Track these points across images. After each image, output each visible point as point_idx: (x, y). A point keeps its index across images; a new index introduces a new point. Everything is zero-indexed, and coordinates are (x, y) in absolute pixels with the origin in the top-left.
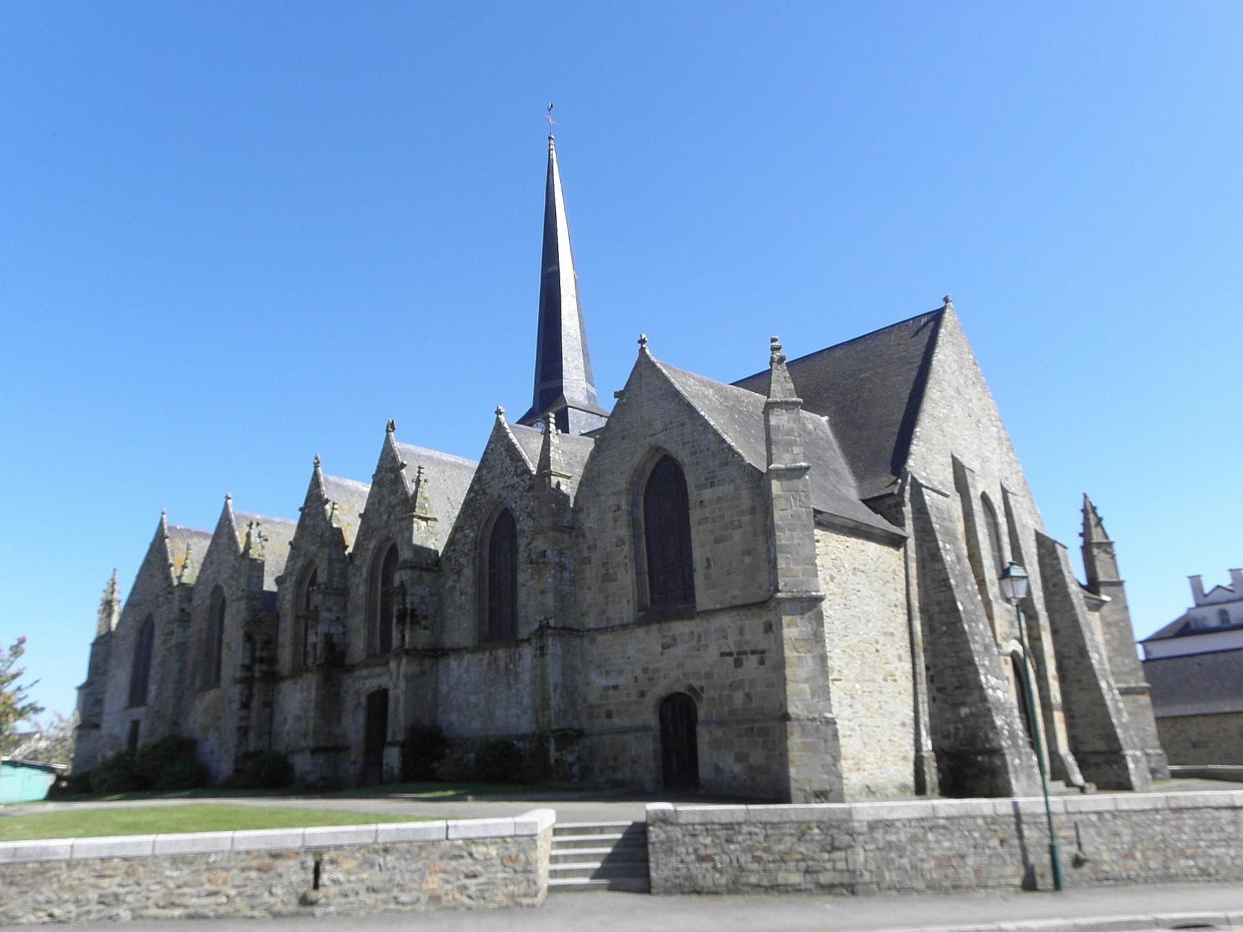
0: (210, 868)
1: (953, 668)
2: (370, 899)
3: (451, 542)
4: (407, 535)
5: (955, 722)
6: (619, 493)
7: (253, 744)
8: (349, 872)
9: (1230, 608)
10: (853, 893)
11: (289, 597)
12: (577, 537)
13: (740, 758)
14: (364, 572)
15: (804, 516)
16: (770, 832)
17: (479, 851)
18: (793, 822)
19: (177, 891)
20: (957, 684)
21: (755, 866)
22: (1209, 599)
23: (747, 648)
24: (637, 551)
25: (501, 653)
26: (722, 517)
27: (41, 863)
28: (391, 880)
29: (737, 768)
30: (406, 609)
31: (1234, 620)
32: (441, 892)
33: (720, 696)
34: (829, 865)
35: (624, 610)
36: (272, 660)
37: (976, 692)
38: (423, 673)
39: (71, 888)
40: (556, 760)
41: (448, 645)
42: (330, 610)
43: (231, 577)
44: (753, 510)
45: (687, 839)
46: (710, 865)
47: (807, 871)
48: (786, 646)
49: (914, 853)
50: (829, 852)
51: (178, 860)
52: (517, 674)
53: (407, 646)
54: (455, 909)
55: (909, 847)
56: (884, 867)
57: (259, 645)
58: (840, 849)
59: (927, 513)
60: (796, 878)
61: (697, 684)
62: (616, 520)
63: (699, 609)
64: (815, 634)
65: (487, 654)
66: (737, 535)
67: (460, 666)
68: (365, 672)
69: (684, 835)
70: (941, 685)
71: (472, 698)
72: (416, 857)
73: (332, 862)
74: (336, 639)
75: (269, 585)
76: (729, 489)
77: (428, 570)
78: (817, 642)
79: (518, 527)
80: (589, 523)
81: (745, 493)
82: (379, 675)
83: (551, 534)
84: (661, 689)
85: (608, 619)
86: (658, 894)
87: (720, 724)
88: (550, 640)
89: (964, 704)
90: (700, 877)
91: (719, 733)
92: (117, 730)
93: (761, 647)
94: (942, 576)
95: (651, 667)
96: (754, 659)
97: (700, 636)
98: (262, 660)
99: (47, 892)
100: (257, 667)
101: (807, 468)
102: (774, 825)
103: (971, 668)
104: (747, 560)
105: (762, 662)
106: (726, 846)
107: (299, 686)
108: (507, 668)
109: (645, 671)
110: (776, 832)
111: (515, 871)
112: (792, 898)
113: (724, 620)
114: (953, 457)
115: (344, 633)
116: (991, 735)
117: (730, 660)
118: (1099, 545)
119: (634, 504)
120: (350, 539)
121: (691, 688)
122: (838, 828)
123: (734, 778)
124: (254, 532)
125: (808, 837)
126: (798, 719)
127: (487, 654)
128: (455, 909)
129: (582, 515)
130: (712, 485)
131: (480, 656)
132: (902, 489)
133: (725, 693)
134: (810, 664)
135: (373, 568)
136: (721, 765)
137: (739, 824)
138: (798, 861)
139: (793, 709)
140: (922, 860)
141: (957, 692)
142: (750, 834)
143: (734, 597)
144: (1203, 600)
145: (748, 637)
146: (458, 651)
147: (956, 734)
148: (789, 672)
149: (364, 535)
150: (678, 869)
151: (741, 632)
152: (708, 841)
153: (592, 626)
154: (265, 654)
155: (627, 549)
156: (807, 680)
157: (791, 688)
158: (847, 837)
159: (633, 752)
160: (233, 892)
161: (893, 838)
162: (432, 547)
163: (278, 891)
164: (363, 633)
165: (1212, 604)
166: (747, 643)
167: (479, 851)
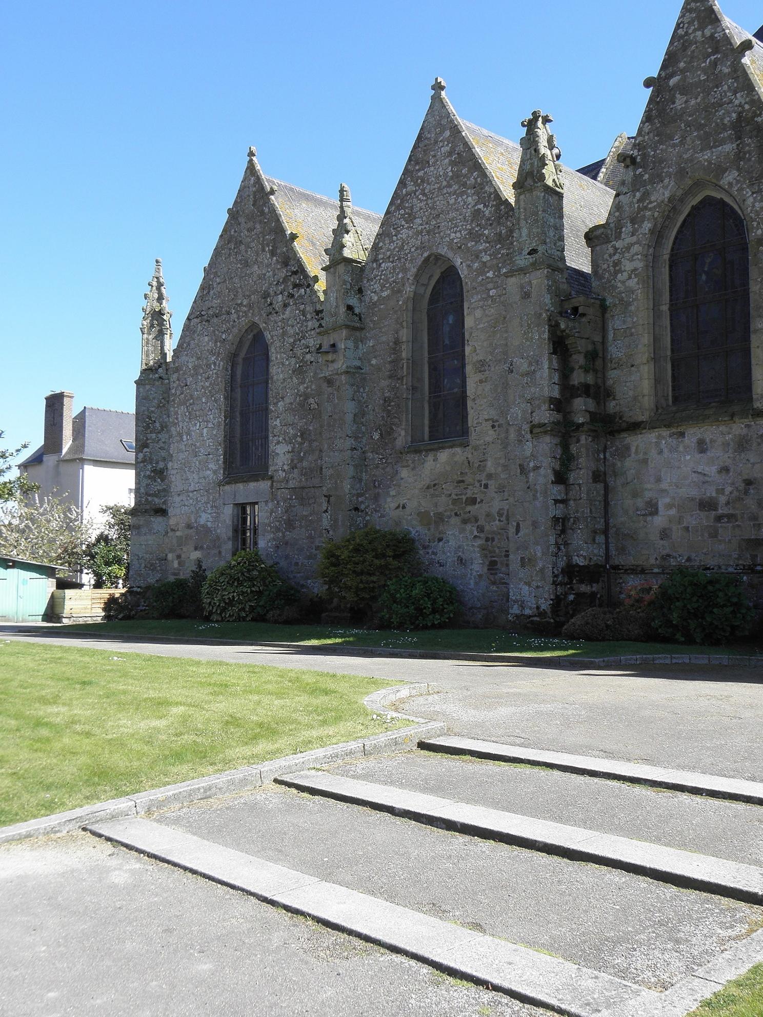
7: (584, 551)
36: (600, 392)
43: (474, 236)
57: (578, 360)
92: (205, 518)
98: (586, 390)
124: (542, 133)
154: (590, 379)
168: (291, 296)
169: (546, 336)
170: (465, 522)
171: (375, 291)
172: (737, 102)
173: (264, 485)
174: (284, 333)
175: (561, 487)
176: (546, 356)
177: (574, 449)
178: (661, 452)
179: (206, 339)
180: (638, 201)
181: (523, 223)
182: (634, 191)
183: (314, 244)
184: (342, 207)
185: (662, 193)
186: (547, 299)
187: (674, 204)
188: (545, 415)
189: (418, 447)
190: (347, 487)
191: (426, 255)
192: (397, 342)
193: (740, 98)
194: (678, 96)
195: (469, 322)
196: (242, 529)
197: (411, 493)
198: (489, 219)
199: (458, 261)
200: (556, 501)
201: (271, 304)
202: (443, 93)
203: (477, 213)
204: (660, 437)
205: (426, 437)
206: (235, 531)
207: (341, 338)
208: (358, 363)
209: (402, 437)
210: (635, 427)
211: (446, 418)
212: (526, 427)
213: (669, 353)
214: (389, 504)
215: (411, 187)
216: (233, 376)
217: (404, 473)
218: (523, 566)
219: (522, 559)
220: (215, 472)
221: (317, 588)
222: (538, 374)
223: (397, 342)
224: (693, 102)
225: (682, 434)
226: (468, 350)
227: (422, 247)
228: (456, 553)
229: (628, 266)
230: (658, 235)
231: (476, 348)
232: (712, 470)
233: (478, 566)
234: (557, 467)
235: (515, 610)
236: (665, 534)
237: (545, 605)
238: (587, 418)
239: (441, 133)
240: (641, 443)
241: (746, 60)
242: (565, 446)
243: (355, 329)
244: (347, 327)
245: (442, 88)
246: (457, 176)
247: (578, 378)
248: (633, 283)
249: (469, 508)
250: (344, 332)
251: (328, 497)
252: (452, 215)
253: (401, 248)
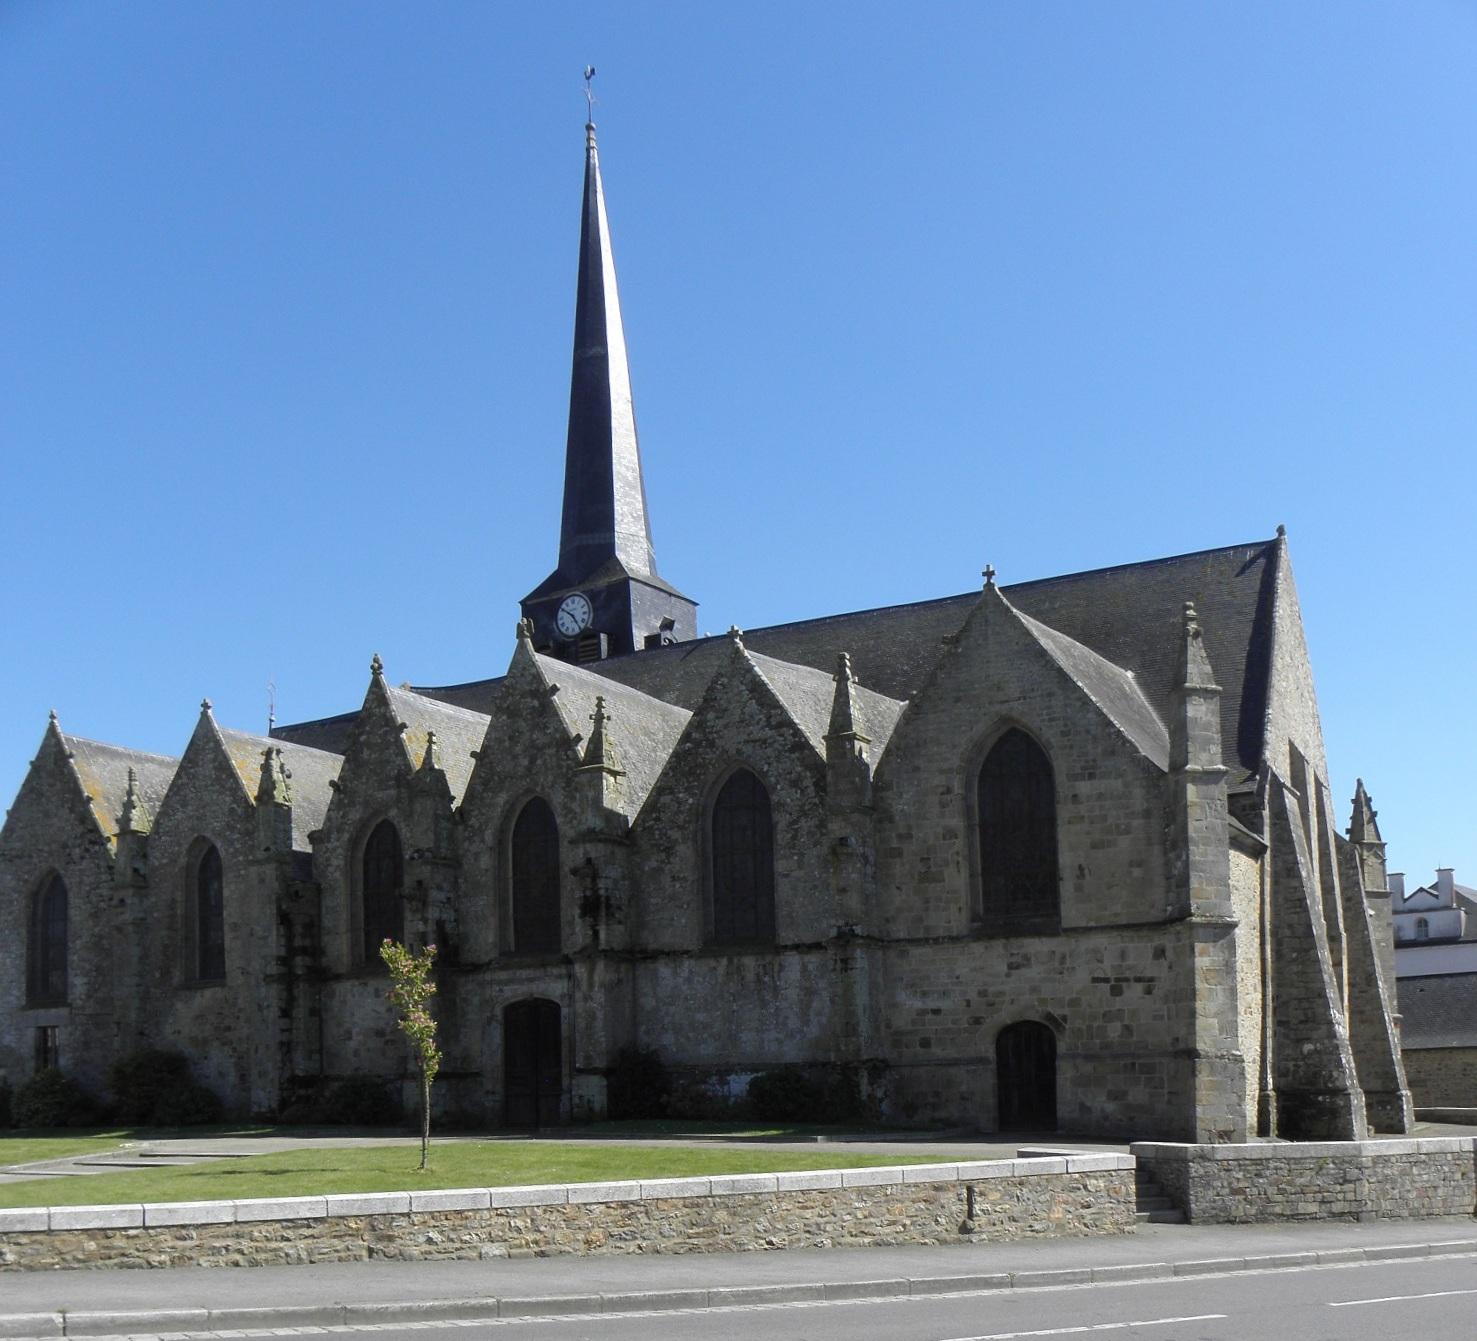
0: (888, 1199)
1: (1300, 1000)
2: (1012, 1227)
3: (650, 808)
4: (591, 794)
5: (1295, 1060)
6: (950, 770)
7: (302, 1066)
8: (994, 1204)
9: (1430, 917)
10: (1358, 1220)
11: (337, 861)
12: (880, 821)
13: (1114, 1096)
14: (489, 836)
15: (1219, 829)
16: (1293, 1167)
17: (1092, 1183)
18: (1312, 1158)
19: (864, 1221)
20: (1303, 1018)
21: (1279, 1198)
22: (1408, 905)
23: (1127, 974)
24: (971, 846)
25: (749, 962)
26: (1104, 818)
27: (756, 1195)
28: (1026, 1210)
29: (1111, 1107)
30: (598, 897)
31: (1432, 933)
32: (1064, 1222)
33: (1090, 1027)
34: (1340, 1196)
35: (955, 918)
36: (316, 951)
37: (1324, 1028)
38: (620, 981)
39: (783, 1219)
40: (869, 1096)
41: (652, 946)
42: (440, 888)
44: (1147, 814)
45: (1222, 1174)
46: (1241, 1197)
47: (1323, 1202)
48: (1197, 977)
49: (1403, 1185)
50: (1341, 1184)
51: (863, 1192)
52: (776, 990)
53: (603, 945)
54: (1076, 1235)
55: (1399, 1180)
56: (1381, 1197)
57: (298, 929)
58: (1350, 1182)
59: (1287, 819)
60: (1313, 1208)
61: (1057, 1012)
62: (943, 805)
63: (1065, 924)
64: (1226, 965)
65: (724, 961)
66: (1124, 842)
67: (675, 974)
68: (503, 975)
69: (1220, 1170)
70: (1284, 1019)
71: (701, 1017)
72: (1044, 1191)
73: (982, 1194)
74: (449, 927)
75: (300, 844)
76: (1117, 785)
77: (620, 844)
78: (1228, 973)
79: (774, 798)
80: (901, 804)
81: (1138, 793)
82: (531, 980)
83: (855, 817)
84: (1005, 1016)
85: (927, 929)
86: (1197, 1224)
87: (1088, 1058)
88: (858, 951)
89: (1308, 1040)
90: (1234, 1208)
91: (1087, 1068)
93: (1148, 974)
94: (1298, 895)
95: (991, 989)
96: (1139, 987)
97: (1063, 957)
98: (304, 951)
99: (763, 1223)
100: (299, 960)
101: (1225, 773)
102: (1297, 1161)
103: (1321, 1001)
104: (1137, 872)
105: (1149, 992)
106: (1256, 1180)
107: (370, 989)
108: (759, 980)
109: (983, 994)
110: (1298, 1167)
111: (1119, 1201)
112: (1307, 1225)
113: (1100, 941)
114: (1291, 744)
115: (455, 921)
116: (1335, 1074)
117: (1106, 987)
118: (1371, 846)
119: (968, 786)
120: (458, 788)
121: (1050, 1017)
122: (1350, 1163)
123: (1106, 1118)
124: (275, 763)
125: (1324, 1171)
126: (1207, 1057)
127: (724, 961)
128: (1076, 1235)
129: (889, 794)
130: (1091, 776)
131: (712, 963)
132: (1262, 788)
133: (1095, 1025)
134: (1221, 998)
135: (501, 832)
136: (1089, 1104)
137: (1267, 1159)
138: (1316, 1192)
139: (1202, 1045)
140: (1409, 1191)
141: (1301, 1026)
142: (1276, 1168)
143: (1116, 915)
144: (1401, 906)
145: (1130, 962)
146: (674, 955)
147: (1296, 1072)
148: (1199, 1005)
149: (486, 783)
150: (1214, 1201)
151: (1123, 955)
152: (1240, 1175)
153: (902, 935)
154: (307, 942)
155: (959, 844)
156: (1216, 1015)
157: (1200, 1022)
158: (1356, 1171)
159: (964, 1088)
160: (908, 1222)
161: (1388, 1171)
162: (621, 812)
163: (942, 1220)
164: (493, 921)
165: (1411, 911)
166: (1129, 968)
167: (1092, 1183)
168: (87, 850)
169: (275, 911)
170: (224, 1044)
171: (157, 859)
172: (398, 762)
173: (64, 1011)
174: (81, 882)
175: (286, 1020)
176: (274, 927)
177: (296, 992)
178: (354, 996)
179: (9, 877)
180: (342, 817)
181: (261, 827)
182: (339, 810)
183: (108, 800)
184: (130, 786)
185: (355, 815)
186: (276, 885)
187: (363, 824)
188: (273, 969)
189: (189, 986)
190: (133, 1015)
191: (196, 835)
192: (174, 901)
193: (399, 761)
194: (365, 749)
195: (226, 893)
196: (44, 1051)
197: (184, 1021)
198: (240, 817)
199: (219, 845)
200: (283, 1031)
201: (69, 855)
202: (210, 711)
203: (232, 810)
204: (353, 986)
205: (197, 976)
206: (38, 1050)
207: (128, 894)
208: (141, 915)
209: (177, 976)
210: (338, 977)
211: (210, 967)
212: (262, 976)
213: (363, 925)
214: (168, 1030)
215: (185, 780)
216: (34, 914)
217: (179, 1005)
218: (260, 1076)
219: (260, 1072)
220: (18, 998)
221: (109, 1097)
222: (270, 939)
223: (174, 901)
224: (373, 756)
225: (366, 984)
226: (225, 913)
227: (192, 829)
228: (217, 1066)
229: (335, 862)
230: (354, 843)
231: (230, 914)
232: (382, 1009)
233: (232, 1078)
234: (284, 1006)
235: (255, 1109)
236: (356, 1053)
237: (274, 1105)
238: (305, 970)
239: (208, 742)
240: (344, 988)
241: (403, 736)
242: (290, 990)
243: (141, 888)
244: (133, 886)
245: (209, 707)
246: (218, 779)
247: (298, 942)
248: (337, 874)
249: (227, 1034)
250: (131, 891)
251: (118, 1024)
252: (214, 808)
253: (177, 827)
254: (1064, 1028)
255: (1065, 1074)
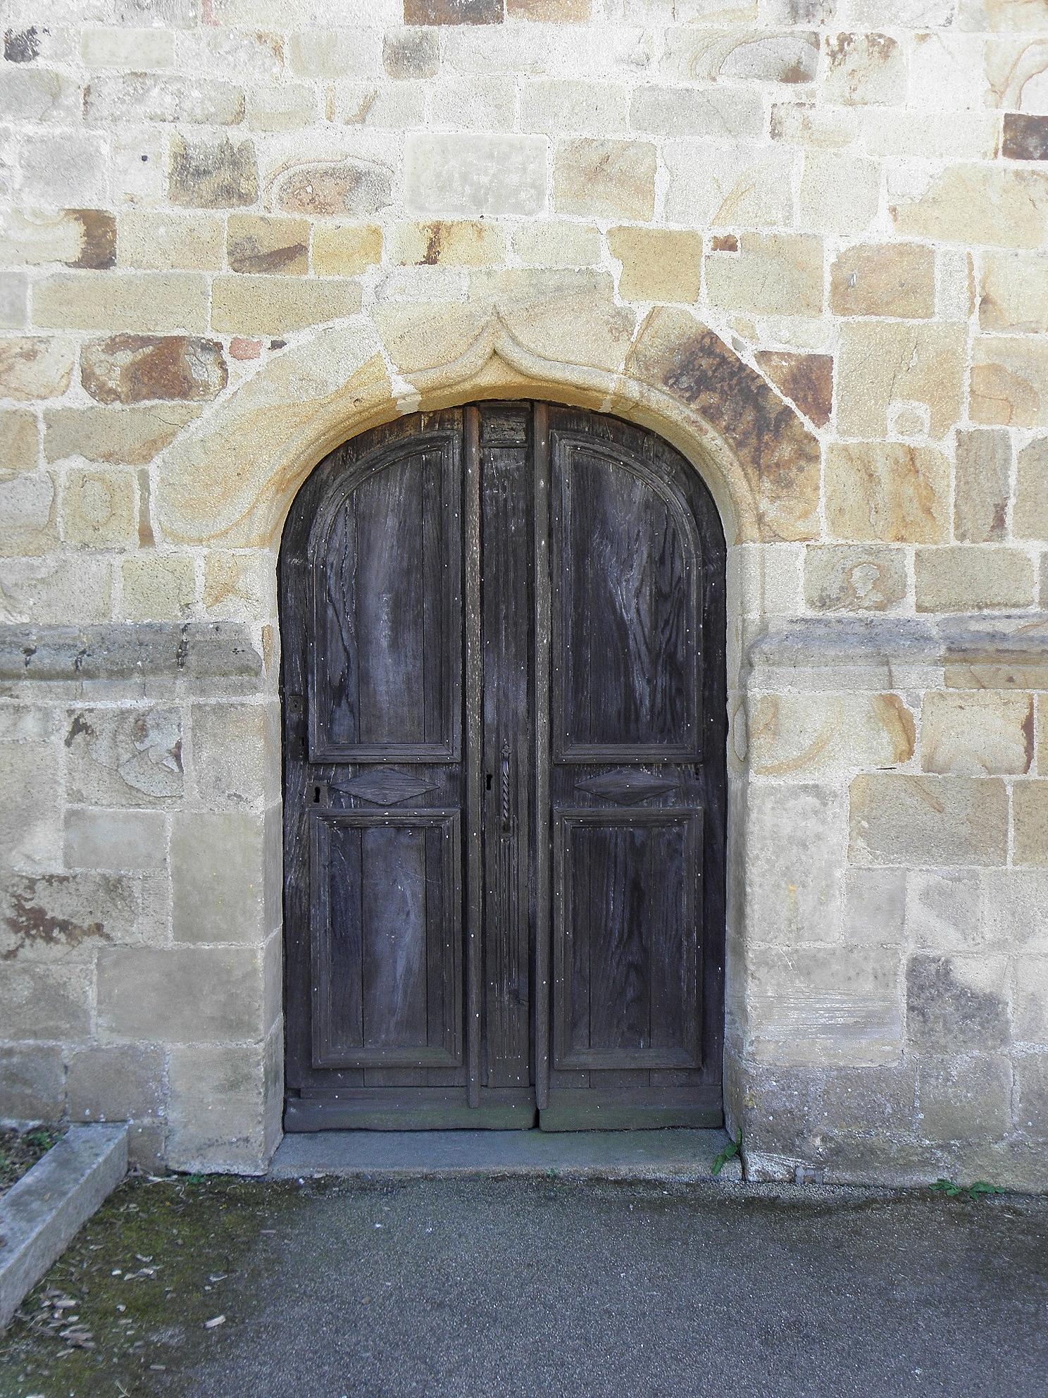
61: (761, 336)
84: (387, 341)
87: (979, 655)
91: (977, 726)
95: (274, 151)
109: (209, 175)
121: (706, 368)
136: (975, 973)
159: (44, 848)
254: (807, 452)
255: (811, 782)
